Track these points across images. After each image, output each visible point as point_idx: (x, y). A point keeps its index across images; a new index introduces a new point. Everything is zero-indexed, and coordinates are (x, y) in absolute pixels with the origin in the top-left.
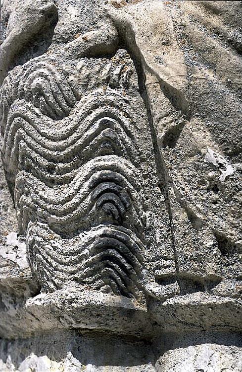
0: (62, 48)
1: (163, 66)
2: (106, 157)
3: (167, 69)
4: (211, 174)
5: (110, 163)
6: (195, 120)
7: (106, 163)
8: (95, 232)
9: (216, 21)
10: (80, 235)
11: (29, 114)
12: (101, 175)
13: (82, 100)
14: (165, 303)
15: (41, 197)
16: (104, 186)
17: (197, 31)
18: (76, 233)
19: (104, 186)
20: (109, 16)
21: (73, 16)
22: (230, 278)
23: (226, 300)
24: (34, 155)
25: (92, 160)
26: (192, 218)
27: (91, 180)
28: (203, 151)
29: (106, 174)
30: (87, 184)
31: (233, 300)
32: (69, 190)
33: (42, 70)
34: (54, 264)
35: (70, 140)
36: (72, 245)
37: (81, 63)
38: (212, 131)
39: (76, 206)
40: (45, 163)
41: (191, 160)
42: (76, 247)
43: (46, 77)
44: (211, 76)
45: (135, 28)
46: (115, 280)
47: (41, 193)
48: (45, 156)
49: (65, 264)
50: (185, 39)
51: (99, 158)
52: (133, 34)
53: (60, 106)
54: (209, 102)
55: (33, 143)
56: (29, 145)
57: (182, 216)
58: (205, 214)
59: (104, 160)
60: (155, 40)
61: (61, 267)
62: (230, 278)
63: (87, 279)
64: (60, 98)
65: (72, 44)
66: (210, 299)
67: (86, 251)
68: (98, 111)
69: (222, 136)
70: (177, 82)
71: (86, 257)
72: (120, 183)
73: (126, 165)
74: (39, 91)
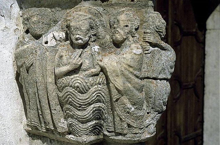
0: (84, 73)
1: (116, 83)
2: (97, 104)
3: (117, 84)
4: (128, 110)
5: (98, 106)
6: (124, 96)
7: (97, 106)
8: (93, 122)
9: (131, 70)
10: (88, 123)
11: (74, 92)
12: (96, 109)
13: (91, 90)
14: (110, 137)
15: (76, 114)
16: (96, 112)
17: (127, 73)
18: (86, 123)
19: (96, 112)
21: (87, 64)
22: (130, 133)
23: (129, 139)
25: (93, 105)
26: (121, 119)
27: (92, 111)
28: (126, 104)
29: (97, 109)
30: (91, 112)
31: (130, 139)
32: (85, 113)
33: (78, 81)
34: (79, 131)
35: (87, 101)
37: (91, 79)
38: (129, 99)
39: (88, 117)
40: (79, 106)
41: (122, 106)
42: (86, 127)
43: (80, 84)
44: (130, 85)
45: (108, 70)
46: (96, 133)
48: (78, 104)
50: (123, 74)
51: (95, 104)
52: (107, 72)
53: (84, 91)
54: (129, 92)
57: (118, 119)
59: (96, 105)
60: (114, 74)
62: (130, 133)
63: (89, 134)
64: (84, 89)
65: (87, 72)
66: (124, 139)
67: (90, 128)
68: (96, 93)
69: (131, 101)
70: (121, 88)
71: (89, 129)
72: (101, 110)
73: (102, 105)
74: (78, 87)
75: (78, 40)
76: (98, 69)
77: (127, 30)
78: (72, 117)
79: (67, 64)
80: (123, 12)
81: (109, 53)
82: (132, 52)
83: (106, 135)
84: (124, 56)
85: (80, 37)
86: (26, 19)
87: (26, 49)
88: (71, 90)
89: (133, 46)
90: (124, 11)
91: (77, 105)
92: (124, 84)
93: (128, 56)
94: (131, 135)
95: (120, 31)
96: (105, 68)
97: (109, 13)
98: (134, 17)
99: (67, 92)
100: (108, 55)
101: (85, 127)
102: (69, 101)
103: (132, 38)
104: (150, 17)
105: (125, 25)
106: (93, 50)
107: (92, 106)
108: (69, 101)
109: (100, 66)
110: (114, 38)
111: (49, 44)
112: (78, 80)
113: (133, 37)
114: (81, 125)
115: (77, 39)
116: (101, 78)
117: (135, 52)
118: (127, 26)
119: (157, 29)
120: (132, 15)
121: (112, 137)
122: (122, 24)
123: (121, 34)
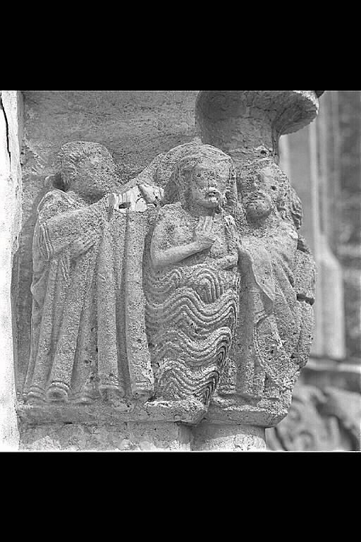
4: (274, 345)
9: (286, 265)
15: (188, 346)
20: (238, 248)
23: (263, 410)
24: (191, 321)
25: (219, 329)
27: (218, 340)
28: (273, 333)
30: (216, 342)
32: (205, 344)
34: (185, 385)
36: (197, 375)
38: (278, 323)
41: (265, 336)
42: (199, 376)
45: (253, 260)
47: (189, 343)
49: (191, 385)
54: (280, 308)
55: (191, 313)
56: (189, 315)
58: (265, 365)
61: (189, 387)
65: (219, 261)
66: (254, 409)
70: (272, 296)
74: (205, 287)
75: (210, 196)
76: (234, 258)
77: (275, 194)
78: (173, 354)
79: (185, 241)
83: (220, 406)
84: (276, 239)
85: (217, 191)
86: (74, 159)
87: (77, 216)
88: (190, 293)
89: (285, 224)
91: (195, 325)
92: (276, 291)
93: (284, 240)
94: (268, 402)
96: (247, 256)
99: (182, 297)
101: (197, 377)
102: (180, 317)
106: (227, 221)
107: (219, 331)
108: (180, 317)
109: (239, 253)
110: (253, 206)
111: (133, 208)
112: (206, 272)
113: (279, 210)
114: (189, 373)
115: (208, 195)
116: (235, 278)
118: (274, 188)
119: (295, 210)
121: (230, 408)
122: (268, 183)
123: (268, 200)
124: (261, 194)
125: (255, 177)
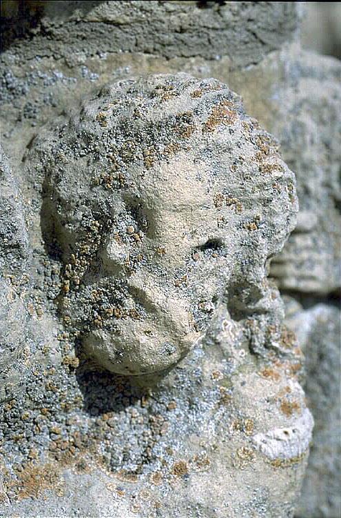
80: (183, 133)
81: (63, 454)
82: (253, 452)
90: (186, 118)
95: (156, 295)
97: (23, 101)
98: (268, 169)
100: (51, 478)
103: (231, 324)
104: (306, 106)
105: (204, 240)
117: (274, 449)
120: (249, 151)
124: (139, 296)
125: (119, 206)
